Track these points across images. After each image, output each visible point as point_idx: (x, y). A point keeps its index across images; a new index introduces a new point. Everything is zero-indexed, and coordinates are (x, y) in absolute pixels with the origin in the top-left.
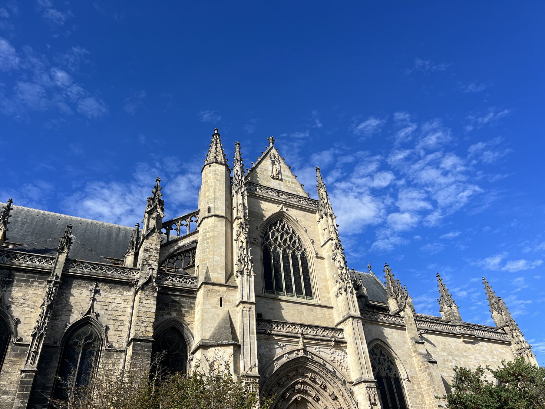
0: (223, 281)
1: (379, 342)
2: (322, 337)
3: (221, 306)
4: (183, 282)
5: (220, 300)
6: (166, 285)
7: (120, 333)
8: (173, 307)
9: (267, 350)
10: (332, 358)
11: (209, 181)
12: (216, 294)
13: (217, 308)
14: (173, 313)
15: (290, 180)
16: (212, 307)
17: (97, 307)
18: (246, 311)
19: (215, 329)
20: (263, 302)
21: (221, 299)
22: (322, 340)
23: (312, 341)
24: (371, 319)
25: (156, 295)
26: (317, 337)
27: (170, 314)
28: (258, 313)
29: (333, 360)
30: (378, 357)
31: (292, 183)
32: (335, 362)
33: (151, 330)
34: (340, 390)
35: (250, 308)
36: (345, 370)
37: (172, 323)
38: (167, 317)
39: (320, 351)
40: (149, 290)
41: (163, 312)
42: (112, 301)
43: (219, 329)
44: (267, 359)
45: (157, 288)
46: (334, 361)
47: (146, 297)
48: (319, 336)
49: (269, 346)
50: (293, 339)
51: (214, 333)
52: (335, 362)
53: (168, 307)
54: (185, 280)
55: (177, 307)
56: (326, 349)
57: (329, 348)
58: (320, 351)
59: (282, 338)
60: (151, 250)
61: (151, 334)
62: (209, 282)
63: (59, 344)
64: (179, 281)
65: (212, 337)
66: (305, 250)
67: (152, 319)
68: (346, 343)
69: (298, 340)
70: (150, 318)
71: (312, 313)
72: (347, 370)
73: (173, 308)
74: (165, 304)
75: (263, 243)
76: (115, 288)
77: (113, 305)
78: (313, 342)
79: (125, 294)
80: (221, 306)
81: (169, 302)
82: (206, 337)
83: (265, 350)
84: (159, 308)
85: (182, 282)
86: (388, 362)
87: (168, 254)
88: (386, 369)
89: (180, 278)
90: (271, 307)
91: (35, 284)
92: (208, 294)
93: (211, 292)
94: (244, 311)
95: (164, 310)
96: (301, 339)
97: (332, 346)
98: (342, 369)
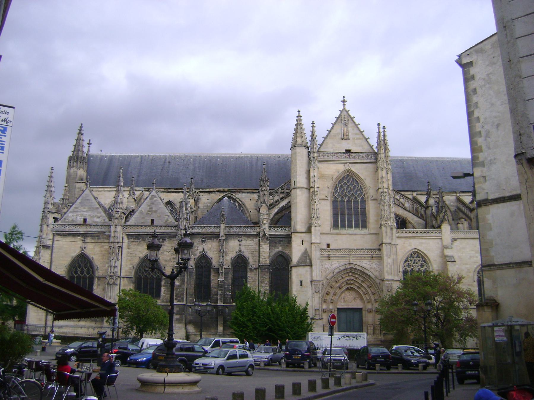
0: (304, 230)
3: (303, 244)
7: (255, 260)
11: (294, 161)
13: (300, 246)
15: (358, 136)
17: (243, 249)
21: (303, 240)
25: (268, 242)
30: (414, 259)
31: (360, 139)
33: (268, 260)
42: (249, 244)
47: (264, 244)
54: (285, 229)
60: (264, 215)
61: (268, 262)
62: (296, 231)
63: (230, 267)
64: (281, 230)
65: (298, 262)
66: (364, 195)
75: (334, 195)
76: (250, 237)
77: (250, 246)
79: (254, 240)
80: (303, 244)
86: (422, 261)
87: (274, 213)
89: (282, 228)
91: (215, 240)
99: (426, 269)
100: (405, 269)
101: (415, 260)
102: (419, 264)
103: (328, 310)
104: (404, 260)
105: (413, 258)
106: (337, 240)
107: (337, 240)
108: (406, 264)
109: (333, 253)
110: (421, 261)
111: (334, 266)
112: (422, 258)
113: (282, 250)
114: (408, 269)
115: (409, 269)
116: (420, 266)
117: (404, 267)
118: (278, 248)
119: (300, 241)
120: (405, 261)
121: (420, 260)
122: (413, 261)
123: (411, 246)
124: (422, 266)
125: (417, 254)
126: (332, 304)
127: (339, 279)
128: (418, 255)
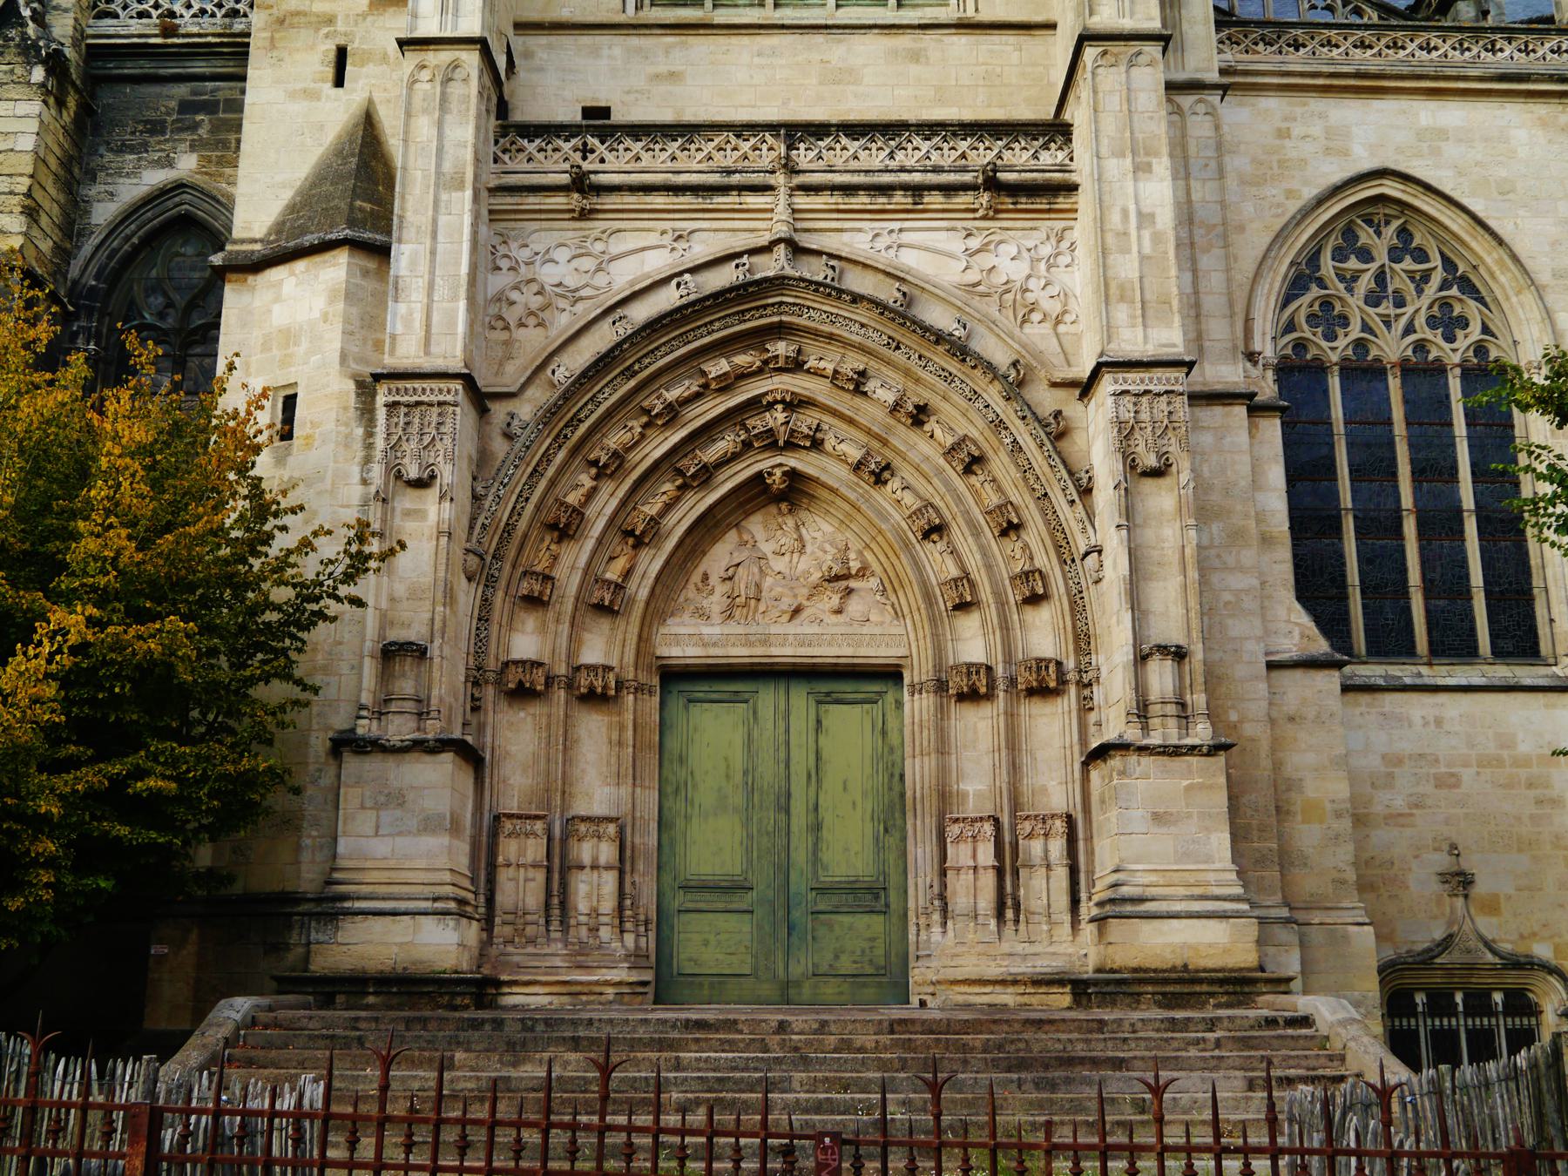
1: (1391, 188)
2: (917, 178)
3: (339, 82)
4: (219, 15)
5: (332, 56)
6: (140, 36)
8: (181, 130)
9: (588, 264)
10: (972, 276)
12: (317, 30)
13: (311, 95)
14: (185, 156)
16: (292, 95)
18: (427, 86)
19: (300, 193)
20: (617, 51)
21: (342, 54)
22: (917, 190)
23: (853, 200)
24: (1345, 69)
26: (887, 178)
27: (169, 163)
28: (589, 104)
29: (978, 284)
30: (1374, 266)
32: (988, 295)
34: (999, 425)
35: (455, 66)
36: (1048, 326)
37: (177, 199)
38: (155, 178)
39: (900, 246)
40: (8, 58)
41: (140, 159)
43: (313, 185)
44: (580, 307)
45: (41, 43)
46: (980, 288)
48: (902, 170)
49: (599, 246)
50: (737, 199)
51: (292, 208)
52: (988, 295)
53: (163, 133)
55: (201, 131)
56: (944, 234)
57: (959, 224)
58: (900, 246)
59: (668, 200)
67: (19, 179)
68: (1072, 188)
69: (769, 199)
70: (10, 175)
71: (914, 70)
72: (1062, 328)
73: (184, 135)
74: (146, 122)
78: (862, 200)
80: (339, 82)
81: (168, 114)
82: (250, 229)
83: (575, 263)
84: (123, 145)
85: (213, 15)
88: (1420, 321)
90: (662, 69)
92: (272, 38)
93: (292, 26)
94: (417, 86)
95: (145, 147)
96: (783, 193)
97: (981, 213)
98: (1024, 322)
99: (1480, 349)
100: (1300, 346)
101: (1380, 278)
102: (1420, 305)
103: (550, 680)
104: (1282, 268)
105: (1366, 255)
106: (673, 76)
107: (673, 76)
108: (1304, 304)
109: (612, 162)
110: (1437, 278)
111: (624, 276)
112: (1449, 264)
113: (200, 180)
114: (1324, 344)
115: (1336, 350)
116: (1432, 322)
117: (1290, 327)
118: (169, 163)
119: (315, 60)
120: (1296, 286)
121: (1426, 277)
122: (1365, 283)
123: (1345, 153)
124: (1449, 324)
125: (1396, 224)
126: (605, 624)
127: (672, 395)
128: (1404, 233)
